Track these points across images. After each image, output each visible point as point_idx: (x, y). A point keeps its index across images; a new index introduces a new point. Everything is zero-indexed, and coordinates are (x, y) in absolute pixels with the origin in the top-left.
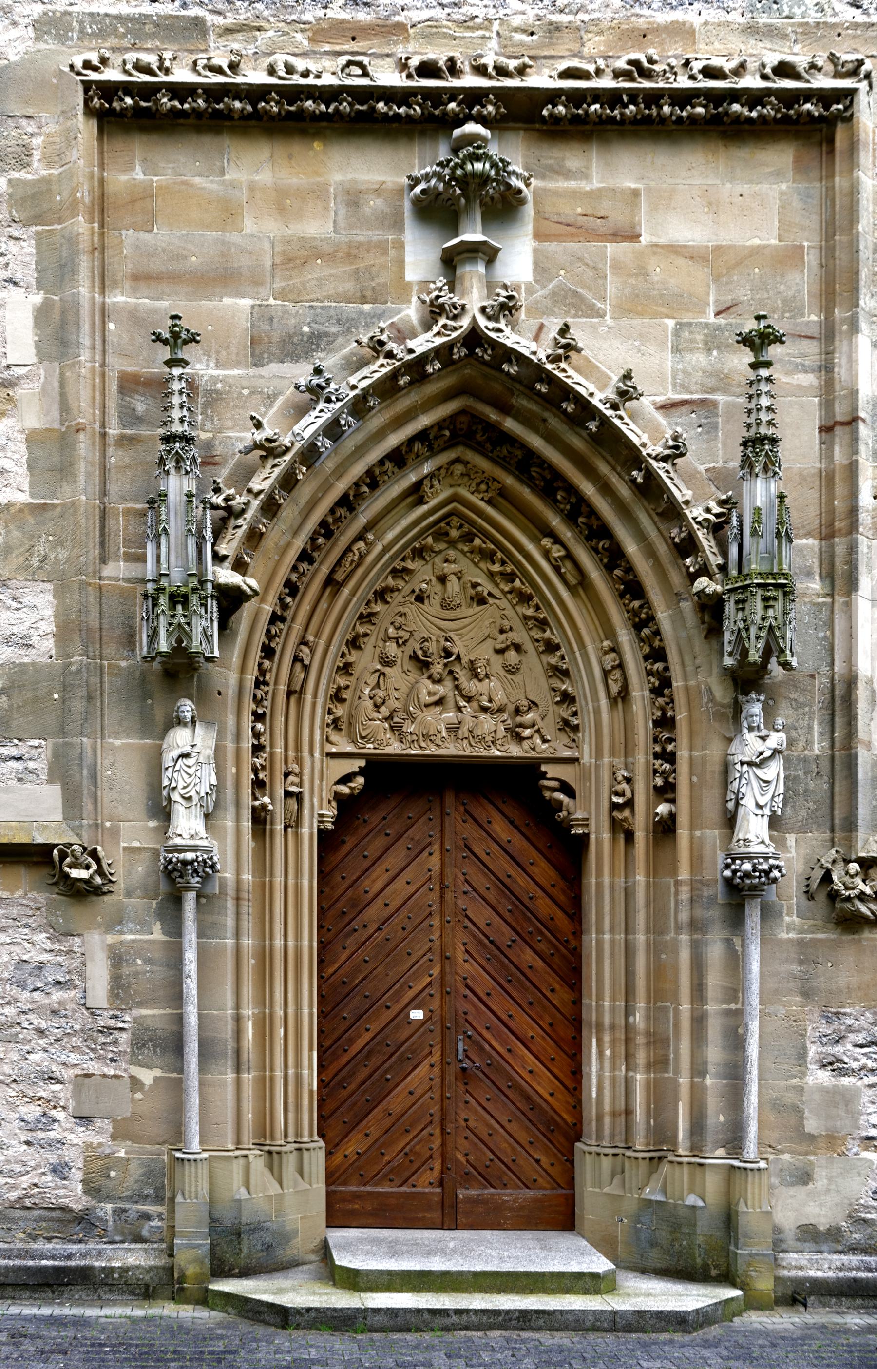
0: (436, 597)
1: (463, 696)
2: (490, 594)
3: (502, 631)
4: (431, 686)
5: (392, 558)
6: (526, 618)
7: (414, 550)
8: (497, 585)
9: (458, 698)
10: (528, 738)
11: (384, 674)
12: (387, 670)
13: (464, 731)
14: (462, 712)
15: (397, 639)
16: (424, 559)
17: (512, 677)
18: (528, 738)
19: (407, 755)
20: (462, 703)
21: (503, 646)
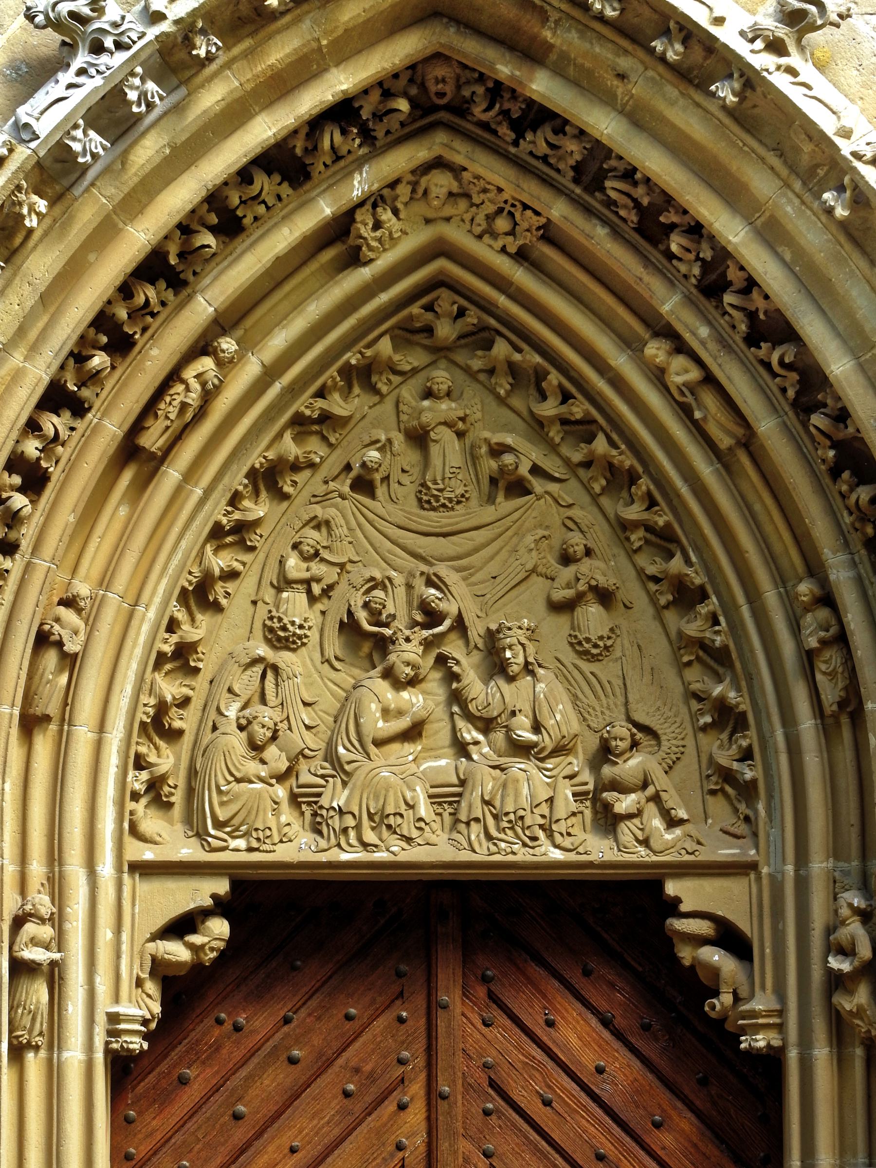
0: (405, 479)
1: (469, 717)
2: (536, 470)
3: (566, 559)
4: (389, 695)
5: (293, 391)
6: (624, 527)
7: (347, 372)
8: (553, 448)
9: (461, 724)
10: (630, 816)
11: (275, 669)
12: (284, 658)
13: (471, 803)
14: (469, 757)
15: (307, 582)
16: (376, 391)
17: (595, 667)
18: (630, 816)
19: (330, 865)
20: (470, 734)
21: (569, 593)
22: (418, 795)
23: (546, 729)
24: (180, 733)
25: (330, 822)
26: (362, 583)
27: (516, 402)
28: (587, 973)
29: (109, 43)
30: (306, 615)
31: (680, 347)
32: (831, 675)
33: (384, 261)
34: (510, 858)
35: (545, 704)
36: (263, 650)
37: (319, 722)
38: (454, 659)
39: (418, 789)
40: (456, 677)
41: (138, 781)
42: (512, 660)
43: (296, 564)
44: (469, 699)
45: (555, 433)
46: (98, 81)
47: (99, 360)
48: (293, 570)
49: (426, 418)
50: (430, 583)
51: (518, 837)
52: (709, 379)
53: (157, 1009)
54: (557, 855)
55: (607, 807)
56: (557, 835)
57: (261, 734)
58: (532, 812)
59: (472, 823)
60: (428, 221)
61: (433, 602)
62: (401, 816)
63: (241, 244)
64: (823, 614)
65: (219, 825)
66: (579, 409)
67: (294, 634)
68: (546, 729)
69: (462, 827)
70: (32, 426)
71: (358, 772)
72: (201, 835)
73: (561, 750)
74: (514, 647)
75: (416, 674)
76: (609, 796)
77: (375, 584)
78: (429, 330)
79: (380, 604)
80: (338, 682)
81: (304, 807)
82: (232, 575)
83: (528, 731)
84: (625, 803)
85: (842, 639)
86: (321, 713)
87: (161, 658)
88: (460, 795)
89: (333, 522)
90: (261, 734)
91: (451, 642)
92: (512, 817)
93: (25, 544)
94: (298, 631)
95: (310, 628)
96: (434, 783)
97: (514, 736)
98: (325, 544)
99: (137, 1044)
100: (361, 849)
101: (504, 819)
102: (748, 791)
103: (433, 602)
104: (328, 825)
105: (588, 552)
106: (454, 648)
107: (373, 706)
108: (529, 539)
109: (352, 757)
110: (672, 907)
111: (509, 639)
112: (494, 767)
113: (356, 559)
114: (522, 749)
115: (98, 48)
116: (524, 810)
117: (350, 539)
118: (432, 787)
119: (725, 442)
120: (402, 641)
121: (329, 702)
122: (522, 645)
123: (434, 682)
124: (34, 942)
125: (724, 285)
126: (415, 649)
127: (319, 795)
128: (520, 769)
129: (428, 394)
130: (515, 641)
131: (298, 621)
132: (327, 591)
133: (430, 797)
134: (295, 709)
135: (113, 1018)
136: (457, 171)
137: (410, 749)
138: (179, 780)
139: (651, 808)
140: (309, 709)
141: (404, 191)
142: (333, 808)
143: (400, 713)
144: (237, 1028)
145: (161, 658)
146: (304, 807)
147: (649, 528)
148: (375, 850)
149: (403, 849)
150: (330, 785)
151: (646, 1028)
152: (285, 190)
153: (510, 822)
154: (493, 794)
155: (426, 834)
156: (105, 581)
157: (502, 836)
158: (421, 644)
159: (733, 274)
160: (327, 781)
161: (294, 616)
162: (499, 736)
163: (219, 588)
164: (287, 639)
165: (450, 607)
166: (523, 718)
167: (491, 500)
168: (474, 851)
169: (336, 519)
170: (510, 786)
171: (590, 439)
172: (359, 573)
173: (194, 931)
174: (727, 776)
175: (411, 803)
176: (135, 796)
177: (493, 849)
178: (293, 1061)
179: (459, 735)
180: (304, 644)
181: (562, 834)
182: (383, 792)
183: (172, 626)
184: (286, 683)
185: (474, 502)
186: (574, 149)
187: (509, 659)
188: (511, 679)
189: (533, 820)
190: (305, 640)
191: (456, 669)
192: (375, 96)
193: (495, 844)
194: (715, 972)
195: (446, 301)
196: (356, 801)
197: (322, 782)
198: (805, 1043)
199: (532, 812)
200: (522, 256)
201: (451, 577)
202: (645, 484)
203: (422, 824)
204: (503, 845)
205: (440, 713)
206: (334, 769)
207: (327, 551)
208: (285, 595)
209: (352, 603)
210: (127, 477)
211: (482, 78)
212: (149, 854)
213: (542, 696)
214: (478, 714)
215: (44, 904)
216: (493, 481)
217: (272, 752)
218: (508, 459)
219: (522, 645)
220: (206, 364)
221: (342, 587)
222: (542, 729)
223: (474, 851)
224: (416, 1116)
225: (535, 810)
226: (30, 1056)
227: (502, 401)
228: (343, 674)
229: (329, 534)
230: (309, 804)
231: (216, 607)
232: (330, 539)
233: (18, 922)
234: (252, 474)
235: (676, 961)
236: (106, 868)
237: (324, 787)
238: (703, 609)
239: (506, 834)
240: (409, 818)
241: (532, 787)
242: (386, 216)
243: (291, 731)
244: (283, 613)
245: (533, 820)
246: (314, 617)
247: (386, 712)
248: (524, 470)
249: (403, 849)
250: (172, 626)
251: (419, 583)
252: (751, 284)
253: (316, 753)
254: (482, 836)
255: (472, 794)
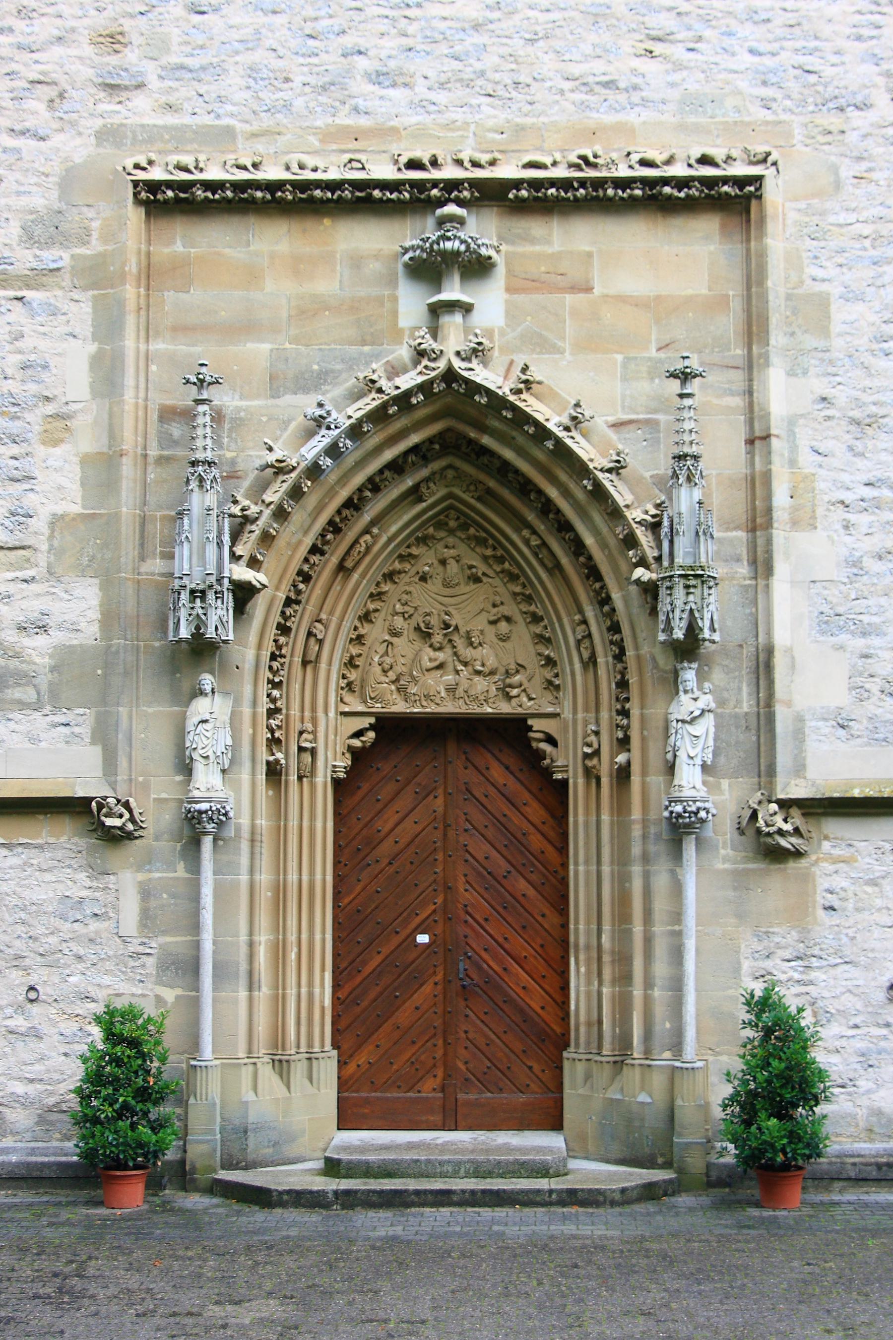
1: (460, 661)
2: (484, 574)
3: (494, 606)
4: (432, 654)
5: (398, 546)
6: (515, 594)
7: (418, 540)
8: (491, 566)
9: (457, 663)
12: (395, 640)
13: (460, 692)
20: (460, 667)
24: (358, 666)
27: (478, 549)
28: (500, 751)
29: (333, 426)
31: (534, 532)
32: (586, 648)
33: (430, 501)
36: (387, 637)
40: (455, 647)
41: (343, 683)
45: (491, 561)
46: (329, 440)
47: (329, 537)
49: (445, 555)
50: (446, 614)
52: (544, 544)
53: (350, 763)
54: (490, 710)
55: (508, 693)
57: (387, 667)
60: (446, 486)
63: (380, 496)
64: (583, 627)
65: (371, 699)
66: (500, 552)
70: (306, 560)
72: (365, 702)
73: (492, 673)
76: (508, 689)
77: (428, 614)
78: (447, 524)
82: (376, 610)
84: (515, 692)
85: (590, 636)
87: (352, 640)
90: (387, 667)
93: (303, 601)
99: (342, 775)
102: (557, 688)
105: (502, 603)
106: (455, 638)
108: (482, 598)
110: (530, 729)
114: (478, 673)
115: (329, 428)
119: (550, 565)
121: (410, 655)
123: (448, 650)
124: (306, 740)
125: (550, 511)
129: (447, 547)
132: (410, 616)
135: (334, 766)
136: (456, 469)
137: (438, 673)
138: (358, 683)
139: (523, 694)
141: (437, 476)
143: (436, 660)
144: (378, 769)
145: (352, 640)
147: (523, 594)
151: (521, 770)
152: (396, 476)
156: (331, 613)
159: (552, 507)
162: (470, 668)
163: (373, 615)
165: (453, 623)
167: (467, 584)
171: (503, 563)
172: (421, 611)
173: (363, 735)
174: (550, 683)
176: (342, 688)
178: (398, 781)
183: (356, 629)
185: (462, 586)
186: (497, 463)
188: (475, 648)
192: (427, 444)
194: (544, 752)
195: (453, 514)
198: (575, 777)
200: (479, 499)
201: (453, 612)
202: (522, 579)
205: (450, 659)
210: (341, 575)
211: (465, 437)
212: (347, 709)
215: (309, 726)
216: (469, 578)
217: (390, 673)
218: (474, 570)
220: (368, 537)
221: (416, 615)
224: (440, 801)
226: (305, 779)
227: (473, 550)
231: (371, 622)
233: (301, 733)
234: (384, 575)
235: (531, 747)
236: (332, 714)
238: (542, 624)
242: (431, 485)
246: (406, 626)
247: (430, 660)
248: (480, 574)
250: (356, 629)
251: (443, 614)
252: (558, 511)
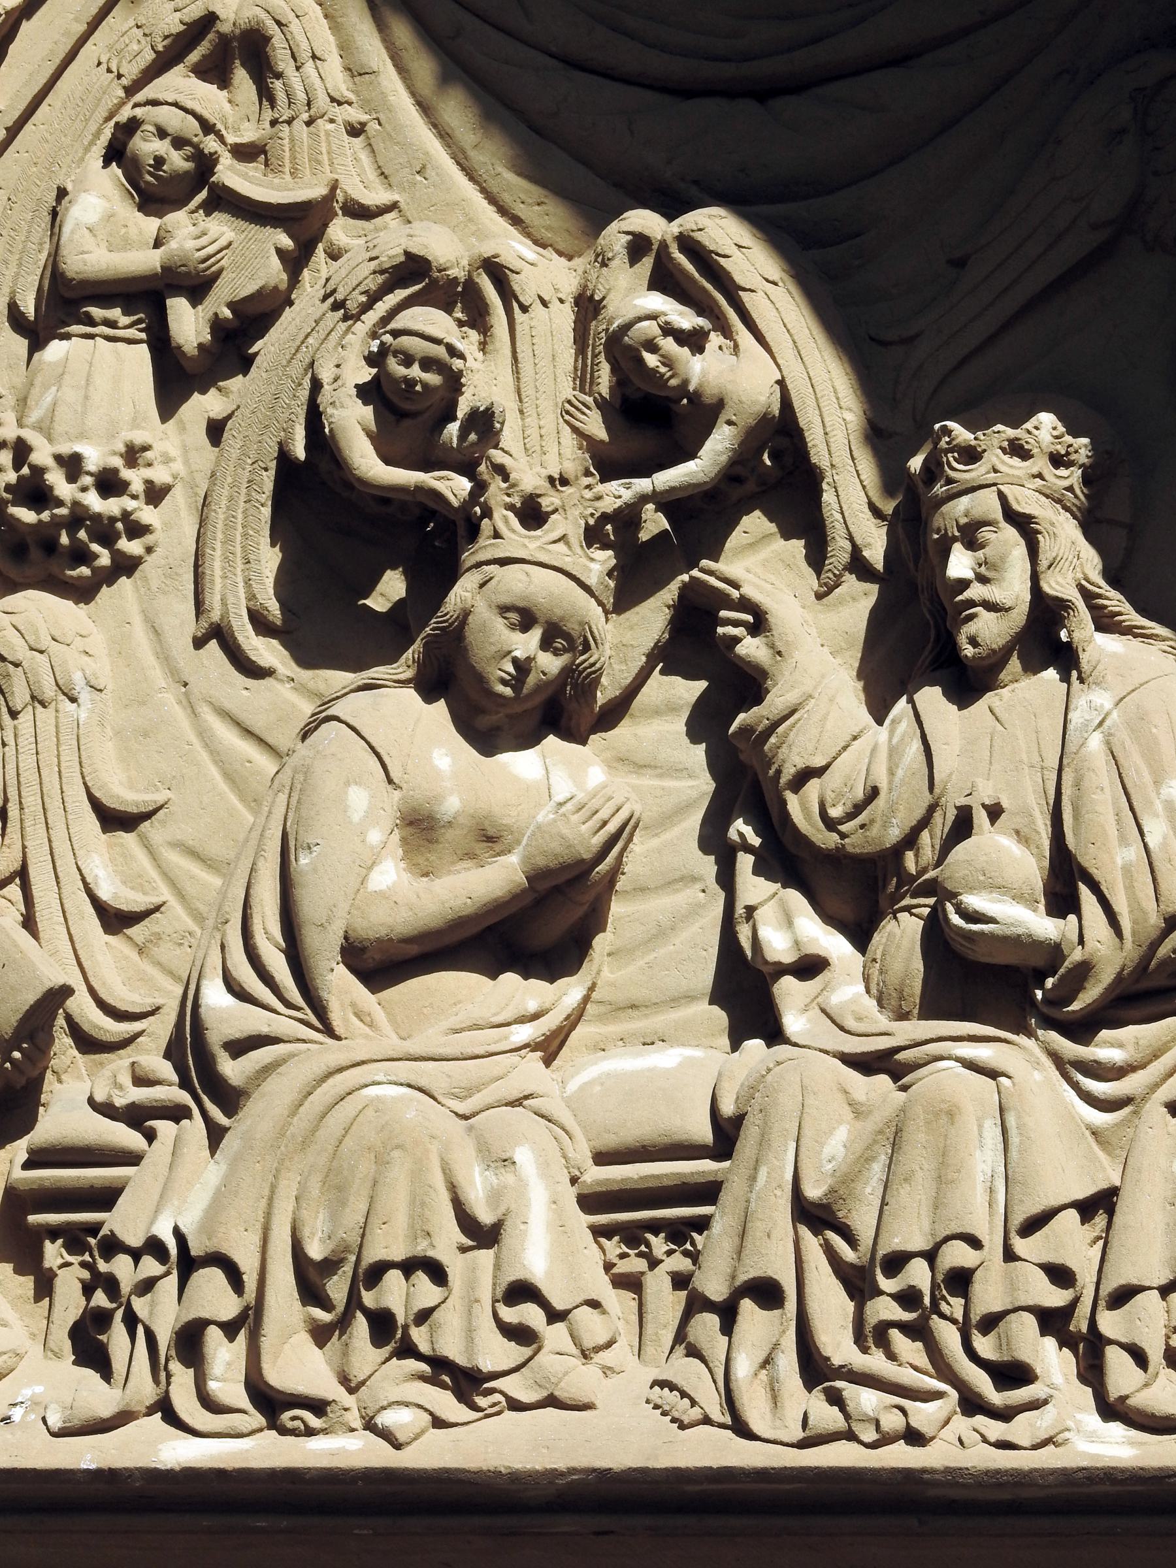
22: (522, 1184)
23: (1095, 887)
25: (140, 1305)
26: (373, 283)
30: (139, 437)
34: (900, 1456)
35: (1102, 777)
37: (164, 894)
38: (745, 604)
39: (523, 1156)
42: (976, 592)
43: (109, 217)
44: (788, 773)
48: (88, 241)
51: (942, 1367)
56: (1117, 1362)
58: (1010, 1256)
59: (747, 1305)
61: (652, 347)
62: (437, 1273)
67: (79, 517)
68: (1095, 887)
69: (707, 1325)
71: (272, 1084)
74: (985, 534)
75: (568, 672)
79: (428, 364)
80: (258, 723)
81: (53, 1253)
83: (1031, 903)
86: (174, 858)
88: (709, 1192)
89: (278, 41)
91: (752, 546)
92: (918, 1274)
94: (94, 502)
95: (155, 494)
96: (610, 1141)
97: (956, 919)
98: (248, 134)
100: (258, 1420)
101: (887, 1284)
103: (652, 347)
104: (131, 1321)
107: (358, 799)
109: (254, 1021)
111: (964, 502)
112: (865, 1064)
113: (375, 196)
116: (974, 1242)
117: (355, 114)
118: (602, 1158)
120: (504, 519)
122: (1024, 524)
126: (560, 555)
127: (106, 1198)
128: (972, 1066)
130: (986, 504)
131: (94, 457)
133: (590, 1202)
134: (59, 833)
140: (128, 839)
142: (155, 1247)
146: (53, 1253)
148: (314, 1422)
149: (439, 1423)
150: (158, 1154)
153: (909, 1298)
154: (848, 1179)
155: (545, 1359)
157: (875, 1362)
158: (593, 536)
160: (150, 1136)
161: (82, 436)
164: (45, 539)
166: (1007, 843)
168: (741, 1429)
169: (295, 27)
170: (918, 1138)
175: (486, 1217)
177: (827, 1416)
179: (744, 934)
180: (126, 566)
181: (1139, 1357)
182: (366, 1167)
184: (25, 718)
187: (964, 584)
189: (1012, 1286)
190: (131, 547)
191: (751, 648)
193: (835, 1399)
196: (249, 1207)
197: (126, 1137)
199: (1010, 1256)
203: (530, 1314)
204: (866, 1400)
206: (185, 1084)
207: (254, 169)
208: (55, 350)
209: (326, 374)
213: (1095, 742)
214: (829, 840)
219: (1024, 524)
222: (1084, 891)
223: (741, 1429)
225: (1020, 1246)
228: (285, 691)
229: (266, 94)
230: (74, 1239)
232: (268, 115)
237: (132, 1159)
239: (892, 1356)
240: (471, 1285)
241: (1014, 1139)
243: (35, 934)
244: (39, 428)
245: (1012, 1286)
249: (439, 1423)
253: (137, 1026)
254: (788, 1362)
255: (753, 1179)
